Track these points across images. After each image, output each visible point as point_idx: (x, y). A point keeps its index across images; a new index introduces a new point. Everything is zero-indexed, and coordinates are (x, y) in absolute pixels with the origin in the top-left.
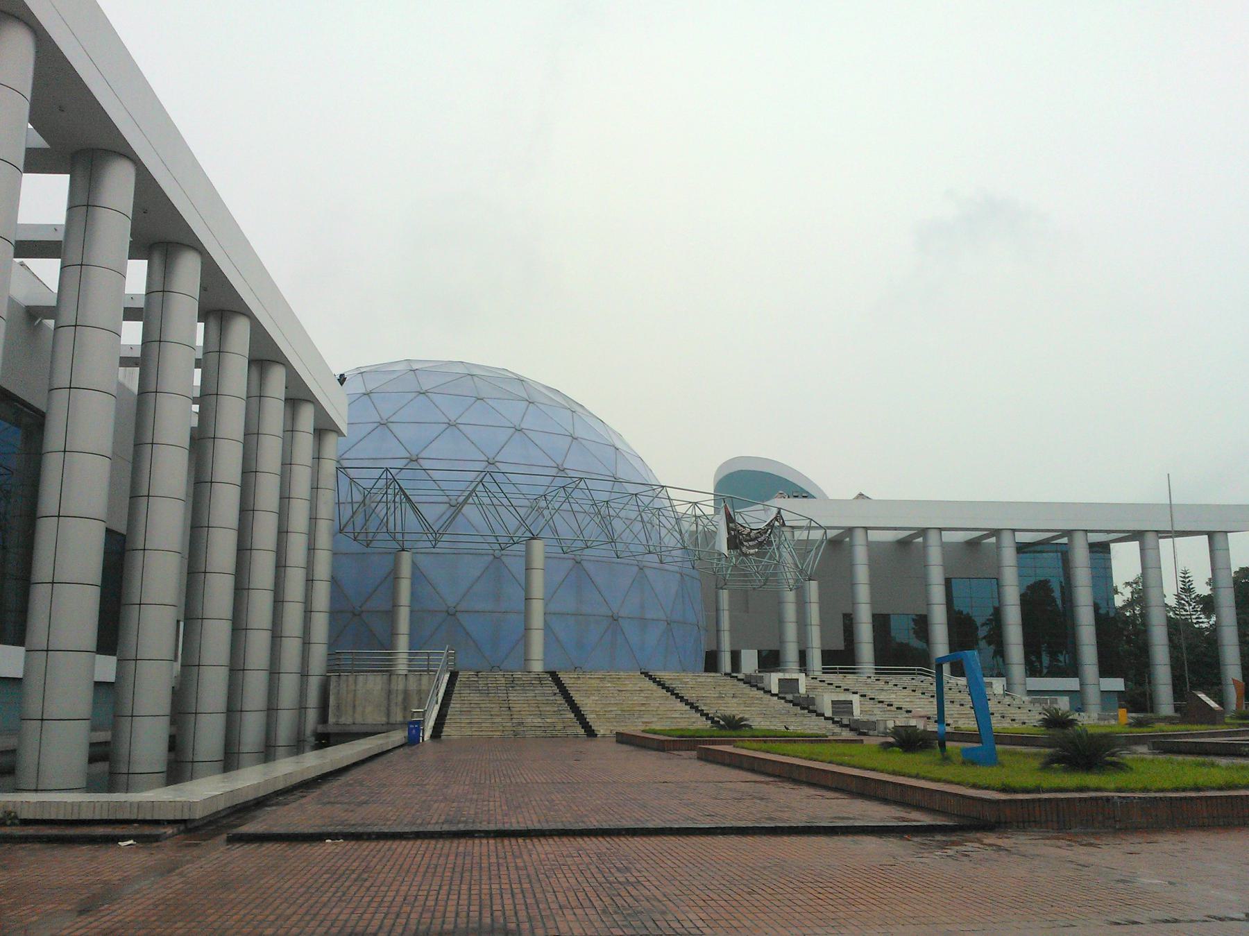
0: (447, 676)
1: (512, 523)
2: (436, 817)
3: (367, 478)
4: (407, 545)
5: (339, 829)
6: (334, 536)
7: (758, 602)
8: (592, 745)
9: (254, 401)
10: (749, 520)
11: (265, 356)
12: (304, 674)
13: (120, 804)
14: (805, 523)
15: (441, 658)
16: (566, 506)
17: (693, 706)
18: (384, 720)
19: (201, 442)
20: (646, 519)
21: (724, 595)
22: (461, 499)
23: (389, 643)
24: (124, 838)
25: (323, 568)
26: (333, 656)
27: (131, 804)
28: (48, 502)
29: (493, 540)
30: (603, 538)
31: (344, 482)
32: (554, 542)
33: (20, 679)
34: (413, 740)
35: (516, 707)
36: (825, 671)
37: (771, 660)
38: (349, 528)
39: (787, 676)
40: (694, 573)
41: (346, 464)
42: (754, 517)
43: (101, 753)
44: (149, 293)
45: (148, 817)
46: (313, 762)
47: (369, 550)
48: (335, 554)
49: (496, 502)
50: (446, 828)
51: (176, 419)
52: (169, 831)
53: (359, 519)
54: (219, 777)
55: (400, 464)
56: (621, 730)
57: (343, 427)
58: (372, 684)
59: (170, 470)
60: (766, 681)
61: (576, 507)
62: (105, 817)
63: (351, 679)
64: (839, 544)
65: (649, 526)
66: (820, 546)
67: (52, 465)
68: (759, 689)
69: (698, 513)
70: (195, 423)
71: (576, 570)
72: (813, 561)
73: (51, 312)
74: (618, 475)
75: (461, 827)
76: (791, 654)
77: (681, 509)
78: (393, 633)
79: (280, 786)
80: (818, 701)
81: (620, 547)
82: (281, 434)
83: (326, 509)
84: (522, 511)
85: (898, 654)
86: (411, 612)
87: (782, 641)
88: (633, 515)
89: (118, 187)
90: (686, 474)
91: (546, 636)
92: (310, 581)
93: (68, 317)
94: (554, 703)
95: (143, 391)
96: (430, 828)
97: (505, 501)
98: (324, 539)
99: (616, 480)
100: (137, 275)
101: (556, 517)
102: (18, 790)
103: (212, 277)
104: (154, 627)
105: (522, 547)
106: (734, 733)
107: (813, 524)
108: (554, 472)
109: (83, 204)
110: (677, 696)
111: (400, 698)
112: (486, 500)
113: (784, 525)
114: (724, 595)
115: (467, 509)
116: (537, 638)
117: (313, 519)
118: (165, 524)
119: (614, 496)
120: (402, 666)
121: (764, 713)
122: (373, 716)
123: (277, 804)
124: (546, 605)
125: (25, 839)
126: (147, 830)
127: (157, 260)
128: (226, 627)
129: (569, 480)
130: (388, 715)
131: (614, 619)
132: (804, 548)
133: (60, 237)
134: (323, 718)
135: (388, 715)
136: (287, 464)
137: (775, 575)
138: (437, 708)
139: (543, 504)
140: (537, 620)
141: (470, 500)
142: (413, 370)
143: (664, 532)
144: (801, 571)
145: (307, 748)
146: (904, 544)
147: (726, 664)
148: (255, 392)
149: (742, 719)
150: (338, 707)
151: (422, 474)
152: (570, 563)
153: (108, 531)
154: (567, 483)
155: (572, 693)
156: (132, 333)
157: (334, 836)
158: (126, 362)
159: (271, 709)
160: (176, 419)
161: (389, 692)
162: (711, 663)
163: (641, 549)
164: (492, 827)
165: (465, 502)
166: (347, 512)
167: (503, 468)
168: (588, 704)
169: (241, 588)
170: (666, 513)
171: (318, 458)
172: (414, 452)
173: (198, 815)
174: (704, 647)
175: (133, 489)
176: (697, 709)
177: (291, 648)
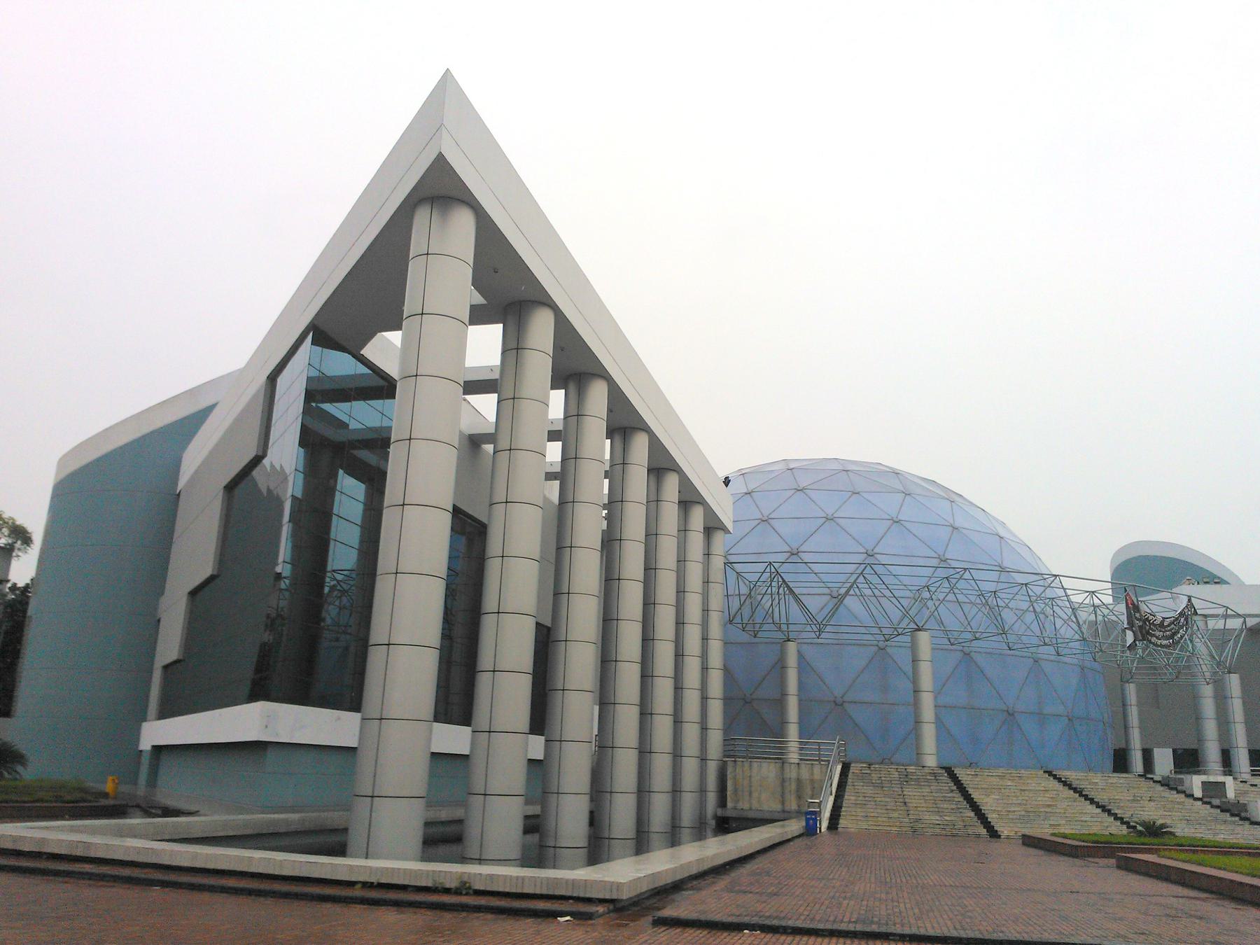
0: (839, 767)
1: (896, 615)
2: (848, 915)
3: (752, 572)
4: (792, 635)
5: (755, 920)
6: (725, 625)
7: (1171, 698)
8: (995, 845)
9: (653, 505)
10: (1154, 609)
11: (662, 466)
12: (703, 759)
13: (557, 881)
14: (1221, 611)
15: (833, 748)
16: (951, 597)
17: (1104, 809)
18: (778, 807)
19: (610, 542)
20: (1038, 610)
21: (1131, 690)
22: (843, 591)
23: (779, 731)
24: (563, 914)
25: (716, 659)
26: (727, 741)
27: (567, 881)
28: (490, 603)
29: (876, 631)
30: (992, 629)
31: (732, 576)
32: (941, 634)
33: (467, 756)
34: (811, 830)
35: (912, 803)
37: (1188, 760)
38: (738, 620)
39: (1212, 779)
40: (1096, 665)
41: (732, 559)
42: (1162, 605)
43: (533, 826)
44: (565, 418)
45: (582, 895)
46: (717, 849)
47: (756, 640)
48: (726, 643)
49: (876, 592)
50: (859, 928)
51: (589, 525)
52: (601, 909)
53: (746, 611)
54: (634, 858)
55: (782, 558)
56: (1027, 832)
57: (729, 525)
58: (766, 771)
59: (586, 570)
60: (1187, 783)
61: (961, 598)
62: (544, 892)
63: (746, 765)
65: (1042, 616)
66: (1238, 636)
67: (493, 568)
68: (1178, 792)
69: (1097, 602)
70: (604, 526)
71: (965, 661)
73: (491, 438)
74: (1005, 564)
75: (875, 928)
76: (1212, 753)
77: (1077, 599)
78: (784, 723)
79: (694, 871)
80: (1251, 807)
81: (1012, 638)
82: (675, 533)
83: (716, 602)
84: (905, 602)
86: (800, 701)
87: (1200, 739)
88: (1025, 606)
89: (541, 330)
90: (1079, 561)
91: (938, 729)
92: (705, 669)
93: (504, 443)
94: (950, 801)
95: (562, 502)
96: (843, 927)
97: (888, 593)
98: (715, 630)
99: (1003, 570)
101: (942, 609)
102: (463, 860)
103: (617, 399)
104: (577, 712)
105: (908, 639)
106: (1156, 841)
107: (1229, 612)
108: (935, 562)
109: (513, 348)
110: (1086, 797)
111: (793, 786)
112: (868, 592)
113: (1196, 613)
114: (1131, 690)
115: (848, 601)
117: (706, 611)
118: (583, 618)
119: (1001, 586)
120: (793, 757)
121: (1187, 819)
122: (769, 804)
123: (692, 888)
124: (936, 698)
125: (478, 909)
126: (582, 907)
127: (572, 387)
128: (635, 710)
129: (952, 571)
130: (783, 803)
132: (1221, 639)
133: (496, 375)
134: (722, 802)
135: (783, 803)
136: (682, 560)
137: (1189, 667)
138: (832, 799)
139: (926, 595)
140: (928, 713)
141: (852, 592)
142: (791, 469)
143: (1059, 623)
144: (1219, 664)
145: (709, 832)
148: (653, 497)
149: (1163, 826)
150: (736, 791)
151: (802, 568)
152: (960, 655)
153: (537, 623)
154: (951, 574)
155: (971, 791)
157: (752, 927)
158: (550, 476)
159: (676, 791)
160: (589, 525)
161: (783, 781)
162: (1120, 762)
163: (1035, 641)
164: (907, 931)
165: (847, 593)
166: (735, 604)
167: (883, 559)
168: (988, 803)
169: (646, 676)
170: (1060, 603)
171: (708, 554)
172: (795, 546)
173: (625, 895)
174: (1112, 743)
175: (556, 589)
176: (1109, 812)
177: (691, 733)
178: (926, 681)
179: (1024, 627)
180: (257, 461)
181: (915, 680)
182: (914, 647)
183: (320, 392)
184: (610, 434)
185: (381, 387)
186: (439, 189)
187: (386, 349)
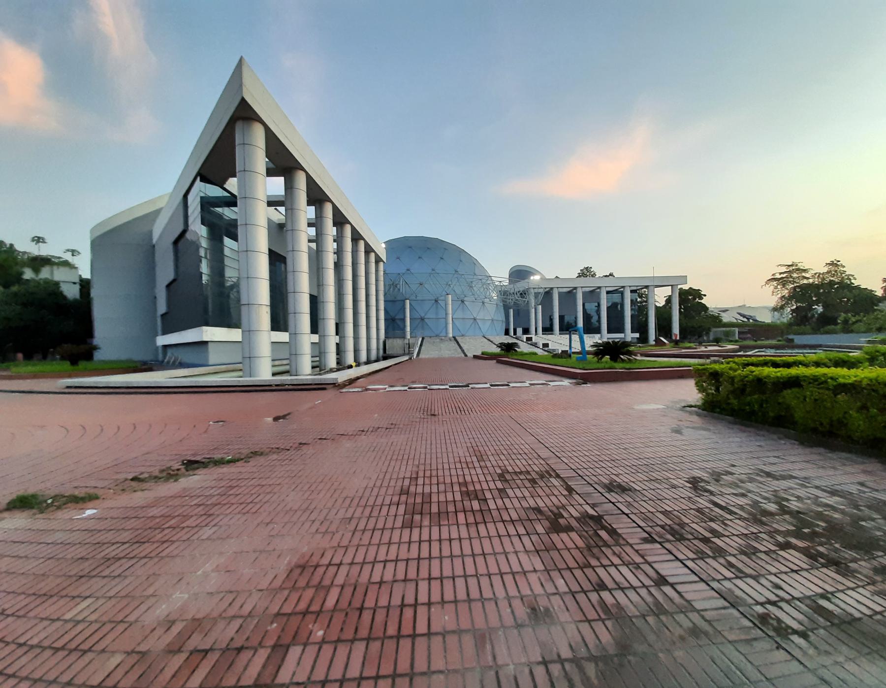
42: (521, 286)
64: (548, 293)
72: (540, 298)
78: (405, 326)
85: (567, 328)
100: (311, 212)
116: (450, 326)
120: (408, 336)
131: (475, 319)
132: (537, 295)
133: (283, 199)
146: (569, 292)
147: (512, 333)
156: (312, 231)
178: (450, 311)
180: (184, 232)
181: (446, 310)
183: (207, 204)
184: (335, 224)
185: (231, 201)
186: (244, 114)
187: (232, 184)
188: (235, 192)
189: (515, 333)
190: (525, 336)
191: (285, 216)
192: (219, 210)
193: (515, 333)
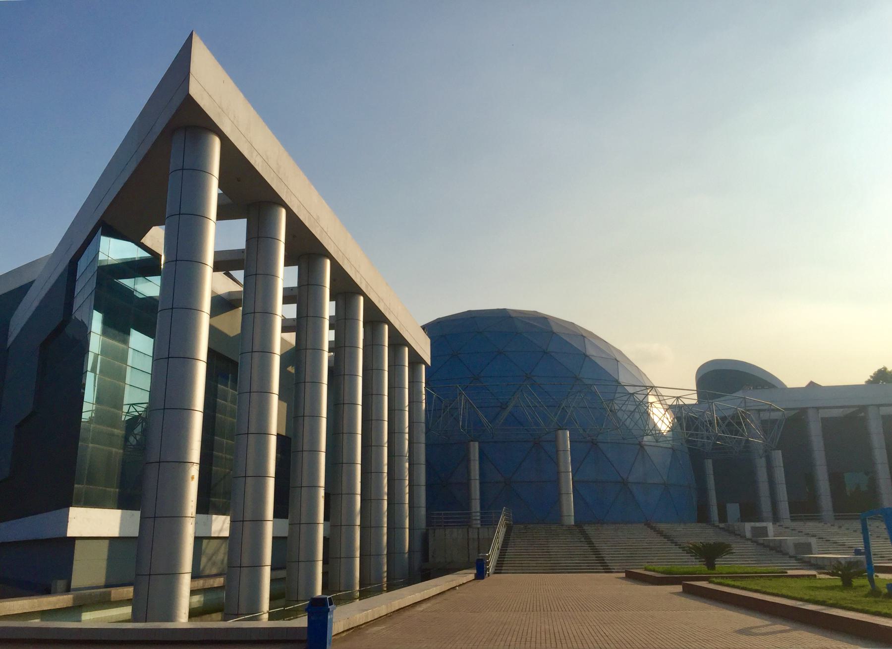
23: (468, 506)
36: (793, 519)
58: (456, 534)
69: (681, 403)
120: (477, 523)
156: (291, 311)
179: (633, 424)
182: (555, 441)
187: (156, 238)
188: (160, 249)
189: (723, 517)
190: (748, 526)
191: (245, 286)
192: (128, 282)
193: (723, 517)
